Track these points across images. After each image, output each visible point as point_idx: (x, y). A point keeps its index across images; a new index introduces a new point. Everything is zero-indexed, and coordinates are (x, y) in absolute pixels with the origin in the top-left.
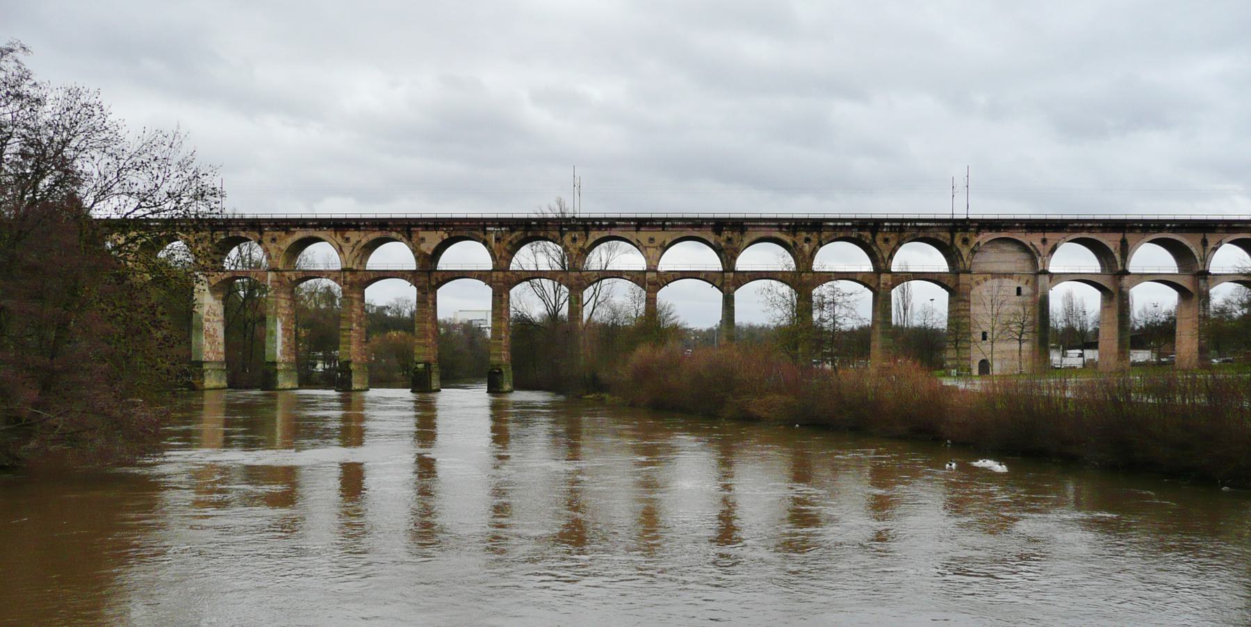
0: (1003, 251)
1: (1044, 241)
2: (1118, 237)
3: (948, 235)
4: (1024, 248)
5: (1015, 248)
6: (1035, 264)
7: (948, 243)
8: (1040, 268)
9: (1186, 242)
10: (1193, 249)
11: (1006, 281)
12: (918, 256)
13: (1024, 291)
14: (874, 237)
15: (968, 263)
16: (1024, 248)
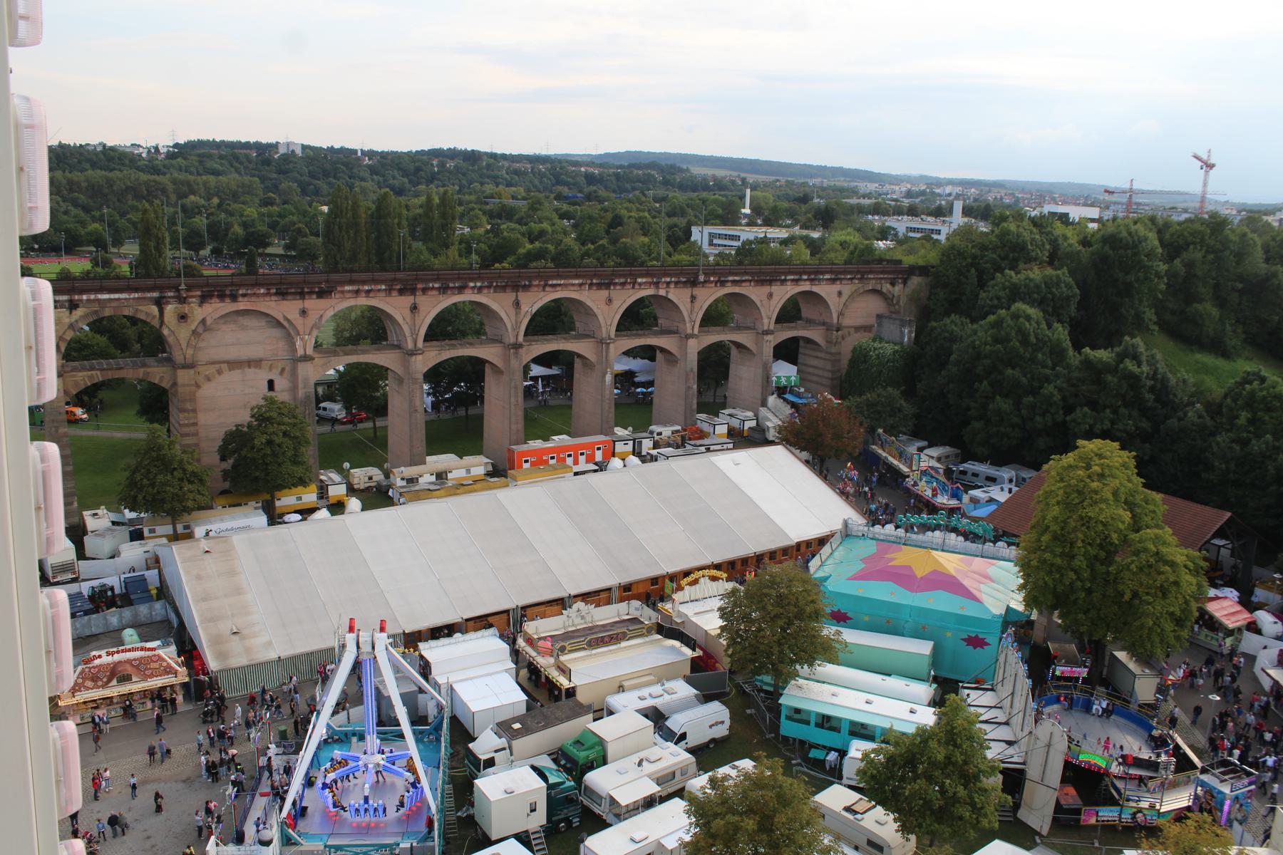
1: (304, 313)
2: (408, 300)
3: (154, 310)
4: (279, 324)
5: (263, 322)
6: (294, 350)
7: (156, 323)
8: (300, 352)
9: (494, 306)
10: (503, 315)
11: (251, 372)
13: (277, 387)
15: (190, 352)
16: (279, 324)
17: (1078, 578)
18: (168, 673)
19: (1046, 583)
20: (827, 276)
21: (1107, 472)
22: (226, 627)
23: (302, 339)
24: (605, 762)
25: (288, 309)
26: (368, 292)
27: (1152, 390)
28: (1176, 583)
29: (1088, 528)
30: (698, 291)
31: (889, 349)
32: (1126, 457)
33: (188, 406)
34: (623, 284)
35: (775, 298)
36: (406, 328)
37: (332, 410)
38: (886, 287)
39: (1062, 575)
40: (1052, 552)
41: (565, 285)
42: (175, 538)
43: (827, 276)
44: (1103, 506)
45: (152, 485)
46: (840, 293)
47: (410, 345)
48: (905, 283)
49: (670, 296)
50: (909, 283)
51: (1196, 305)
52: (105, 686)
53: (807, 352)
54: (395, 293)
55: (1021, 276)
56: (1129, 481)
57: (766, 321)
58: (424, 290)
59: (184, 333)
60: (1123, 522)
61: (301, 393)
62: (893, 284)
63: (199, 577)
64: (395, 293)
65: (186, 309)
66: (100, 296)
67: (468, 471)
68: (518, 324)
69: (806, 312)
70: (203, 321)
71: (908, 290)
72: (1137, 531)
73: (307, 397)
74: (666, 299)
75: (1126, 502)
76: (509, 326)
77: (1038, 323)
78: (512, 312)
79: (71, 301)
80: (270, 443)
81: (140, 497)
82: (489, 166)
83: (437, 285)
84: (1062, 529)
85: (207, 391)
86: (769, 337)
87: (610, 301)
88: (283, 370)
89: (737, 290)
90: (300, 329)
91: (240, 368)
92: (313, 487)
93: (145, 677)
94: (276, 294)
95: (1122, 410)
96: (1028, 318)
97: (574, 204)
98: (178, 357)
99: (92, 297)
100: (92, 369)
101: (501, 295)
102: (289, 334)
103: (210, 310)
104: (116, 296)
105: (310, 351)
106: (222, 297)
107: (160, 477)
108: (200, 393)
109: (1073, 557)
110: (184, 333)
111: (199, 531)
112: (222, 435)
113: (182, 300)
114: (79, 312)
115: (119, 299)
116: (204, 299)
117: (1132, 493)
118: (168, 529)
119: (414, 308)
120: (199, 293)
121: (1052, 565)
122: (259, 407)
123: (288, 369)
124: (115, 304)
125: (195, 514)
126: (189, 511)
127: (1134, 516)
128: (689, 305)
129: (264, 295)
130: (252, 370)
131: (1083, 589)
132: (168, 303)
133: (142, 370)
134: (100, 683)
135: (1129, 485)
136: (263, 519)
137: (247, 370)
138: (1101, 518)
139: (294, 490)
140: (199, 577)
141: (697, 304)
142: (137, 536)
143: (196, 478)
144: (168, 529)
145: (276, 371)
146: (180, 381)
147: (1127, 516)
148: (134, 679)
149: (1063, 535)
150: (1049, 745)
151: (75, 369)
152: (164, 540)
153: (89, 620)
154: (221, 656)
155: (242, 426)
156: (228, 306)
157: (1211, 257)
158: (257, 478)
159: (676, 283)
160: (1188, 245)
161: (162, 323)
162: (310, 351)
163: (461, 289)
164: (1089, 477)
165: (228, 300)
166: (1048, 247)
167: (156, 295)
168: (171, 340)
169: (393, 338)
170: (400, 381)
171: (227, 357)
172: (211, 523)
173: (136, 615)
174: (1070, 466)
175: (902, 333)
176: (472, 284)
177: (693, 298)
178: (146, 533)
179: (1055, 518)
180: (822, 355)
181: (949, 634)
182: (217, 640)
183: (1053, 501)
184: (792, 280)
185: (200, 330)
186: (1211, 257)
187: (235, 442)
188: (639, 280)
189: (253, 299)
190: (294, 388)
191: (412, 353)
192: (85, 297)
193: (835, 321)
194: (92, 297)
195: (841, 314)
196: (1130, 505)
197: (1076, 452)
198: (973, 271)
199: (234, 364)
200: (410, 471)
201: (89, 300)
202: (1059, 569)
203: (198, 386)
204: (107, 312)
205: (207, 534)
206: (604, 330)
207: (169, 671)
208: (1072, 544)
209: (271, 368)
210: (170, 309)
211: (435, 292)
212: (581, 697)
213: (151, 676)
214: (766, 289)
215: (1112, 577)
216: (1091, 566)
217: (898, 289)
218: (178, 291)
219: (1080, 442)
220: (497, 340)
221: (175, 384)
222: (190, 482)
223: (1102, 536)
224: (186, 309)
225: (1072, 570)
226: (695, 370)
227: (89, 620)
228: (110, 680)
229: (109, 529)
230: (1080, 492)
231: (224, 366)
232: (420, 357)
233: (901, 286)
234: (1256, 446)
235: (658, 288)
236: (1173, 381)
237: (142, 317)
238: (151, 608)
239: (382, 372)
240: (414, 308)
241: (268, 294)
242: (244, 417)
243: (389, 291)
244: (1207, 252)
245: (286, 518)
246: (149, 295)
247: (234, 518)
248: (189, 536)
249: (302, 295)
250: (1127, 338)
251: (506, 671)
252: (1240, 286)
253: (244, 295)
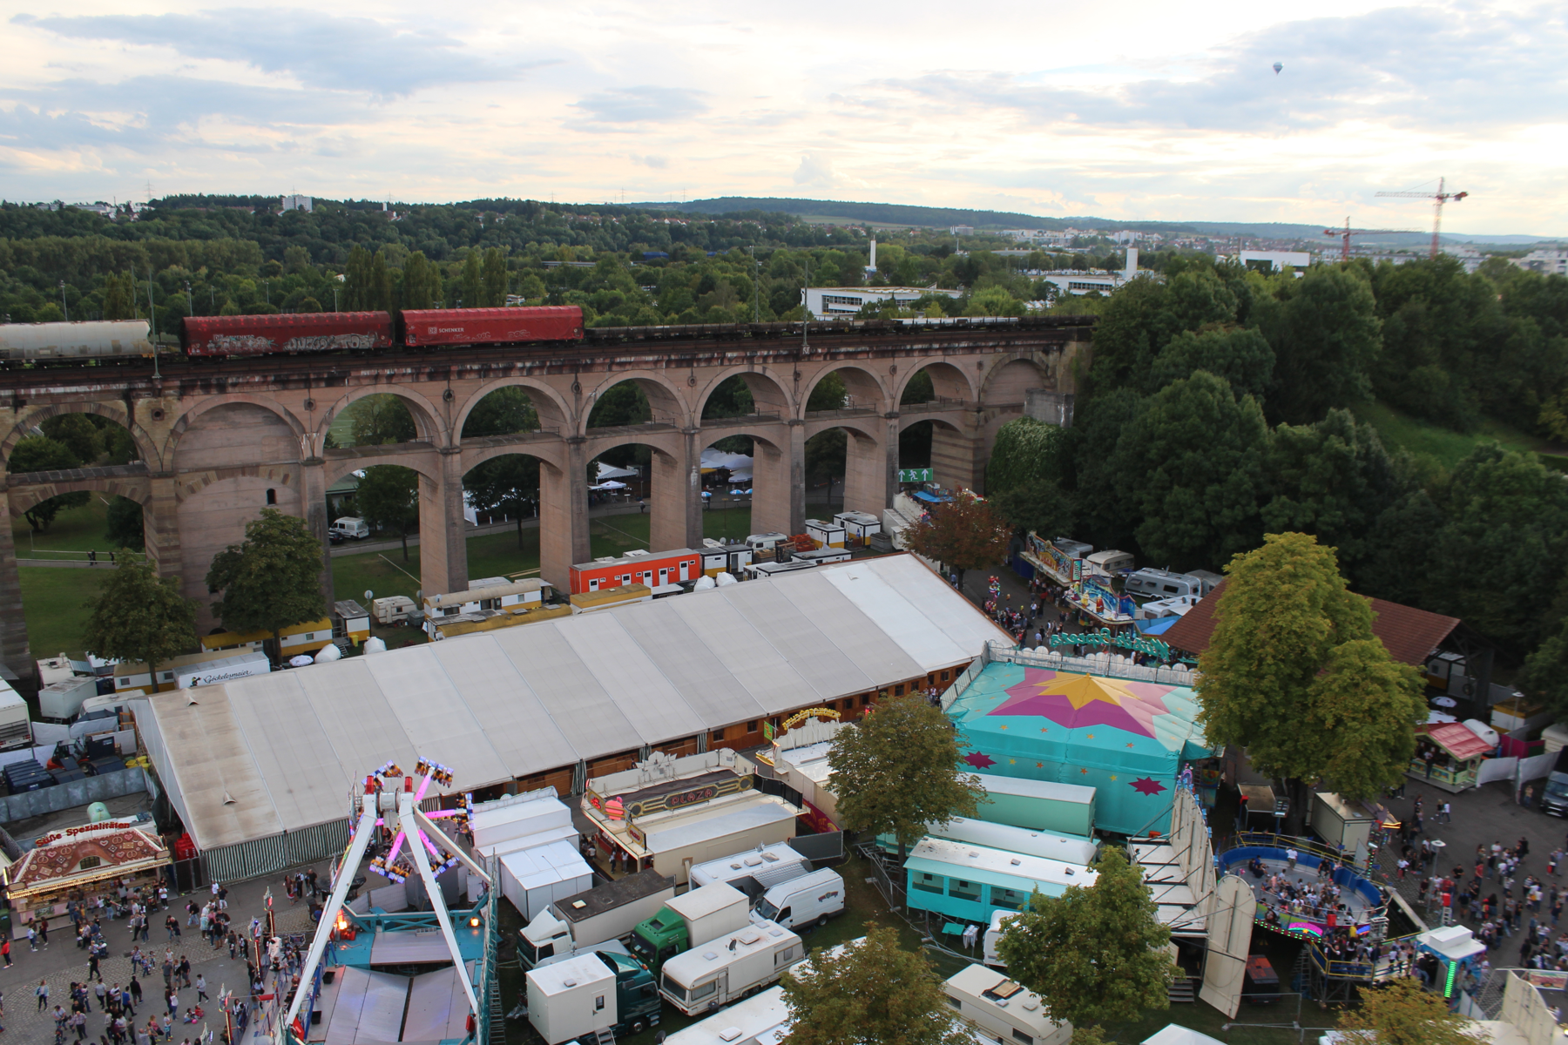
0: (235, 426)
1: (310, 405)
2: (440, 386)
3: (122, 405)
4: (278, 420)
5: (259, 418)
7: (124, 421)
8: (307, 454)
9: (549, 391)
10: (559, 401)
11: (245, 481)
13: (279, 497)
15: (168, 457)
16: (278, 420)
17: (1270, 703)
18: (145, 855)
19: (1230, 710)
20: (964, 344)
21: (1300, 571)
22: (217, 795)
23: (309, 438)
24: (689, 946)
25: (290, 401)
26: (390, 377)
27: (1364, 472)
28: (1387, 705)
29: (1279, 640)
30: (802, 367)
31: (1041, 433)
32: (1326, 552)
33: (168, 525)
34: (709, 360)
35: (900, 373)
36: (438, 421)
37: (351, 527)
38: (1038, 356)
39: (1250, 699)
40: (1237, 671)
41: (638, 363)
42: (155, 689)
43: (964, 344)
44: (1296, 613)
45: (124, 624)
46: (980, 365)
47: (444, 442)
48: (1061, 350)
49: (769, 374)
50: (1067, 350)
51: (1420, 368)
52: (65, 873)
53: (942, 438)
54: (423, 378)
55: (1203, 337)
56: (1329, 581)
57: (888, 401)
58: (461, 374)
59: (160, 434)
60: (1322, 632)
61: (308, 506)
62: (1046, 352)
63: (183, 736)
64: (423, 378)
65: (162, 404)
66: (52, 390)
67: (521, 597)
68: (579, 412)
69: (940, 390)
70: (184, 418)
71: (1065, 359)
72: (1338, 643)
73: (317, 510)
74: (763, 377)
75: (1325, 608)
76: (568, 416)
77: (1223, 394)
78: (571, 397)
79: (15, 397)
80: (270, 567)
81: (108, 639)
82: (548, 220)
83: (476, 367)
84: (1248, 642)
85: (192, 504)
86: (895, 422)
87: (693, 381)
88: (286, 477)
89: (851, 363)
90: (307, 425)
91: (232, 475)
92: (327, 622)
93: (116, 861)
94: (274, 382)
95: (1328, 499)
96: (1212, 389)
97: (655, 264)
98: (152, 464)
99: (43, 391)
100: (45, 481)
101: (557, 378)
102: (292, 432)
103: (192, 404)
104: (73, 389)
105: (319, 453)
106: (207, 388)
107: (134, 613)
108: (183, 508)
109: (1262, 677)
110: (160, 434)
111: (184, 680)
112: (211, 560)
113: (157, 393)
114: (26, 411)
115: (77, 393)
116: (184, 391)
117: (1333, 596)
118: (146, 679)
119: (448, 396)
120: (178, 383)
121: (1237, 687)
122: (257, 524)
123: (291, 476)
124: (70, 400)
125: (178, 659)
126: (171, 655)
127: (1336, 625)
128: (792, 384)
129: (258, 384)
130: (247, 478)
131: (1276, 716)
132: (139, 396)
133: (108, 482)
134: (59, 870)
135: (1330, 587)
136: (265, 663)
137: (240, 478)
138: (1294, 627)
139: (303, 626)
140: (183, 736)
141: (802, 383)
142: (105, 688)
143: (178, 614)
144: (146, 679)
145: (277, 479)
146: (155, 493)
147: (1326, 624)
148: (103, 863)
149: (1249, 651)
150: (1234, 907)
151: (23, 482)
152: (140, 693)
153: (46, 794)
154: (212, 831)
155: (236, 547)
156: (215, 399)
157: (1437, 308)
158: (256, 613)
159: (776, 357)
160: (1409, 294)
161: (132, 421)
162: (319, 453)
163: (506, 371)
164: (1279, 578)
165: (214, 391)
166: (1236, 301)
167: (123, 386)
168: (143, 442)
169: (423, 435)
170: (434, 487)
171: (215, 463)
172: (199, 669)
173: (105, 786)
174: (1256, 566)
175: (1058, 412)
176: (519, 365)
177: (797, 375)
178: (118, 685)
179: (1238, 629)
180: (961, 442)
181: (1114, 778)
182: (206, 813)
183: (1237, 609)
184: (921, 350)
185: (181, 430)
186: (1437, 308)
187: (228, 565)
188: (729, 355)
189: (246, 389)
190: (298, 501)
191: (447, 452)
192: (33, 391)
193: (975, 399)
194: (43, 391)
195: (982, 391)
196: (1330, 612)
197: (1263, 548)
198: (1144, 333)
199: (224, 472)
200: (451, 599)
201: (38, 395)
202: (1246, 691)
203: (179, 499)
204: (62, 410)
205: (195, 683)
206: (687, 417)
207: (147, 851)
208: (1261, 661)
209: (270, 475)
210: (141, 403)
211: (473, 376)
212: (659, 867)
213: (124, 859)
214: (887, 363)
215: (1310, 701)
216: (1284, 688)
217: (1052, 358)
218: (151, 381)
219: (1268, 537)
220: (554, 435)
221: (149, 498)
222: (171, 619)
223: (1298, 650)
224: (162, 404)
225: (1262, 692)
226: (803, 464)
227: (46, 794)
228: (72, 865)
229: (70, 681)
230: (1268, 597)
231: (212, 474)
232: (457, 458)
233: (1056, 354)
234: (1492, 538)
235: (752, 363)
236: (1390, 462)
237: (106, 414)
238: (124, 777)
239: (411, 477)
240: (448, 396)
241: (265, 383)
242: (239, 537)
243: (416, 376)
244: (1433, 302)
245: (293, 661)
246: (114, 387)
247: (228, 663)
248: (172, 686)
249: (307, 383)
250: (1332, 410)
251: (567, 839)
252: (1473, 343)
253: (234, 385)
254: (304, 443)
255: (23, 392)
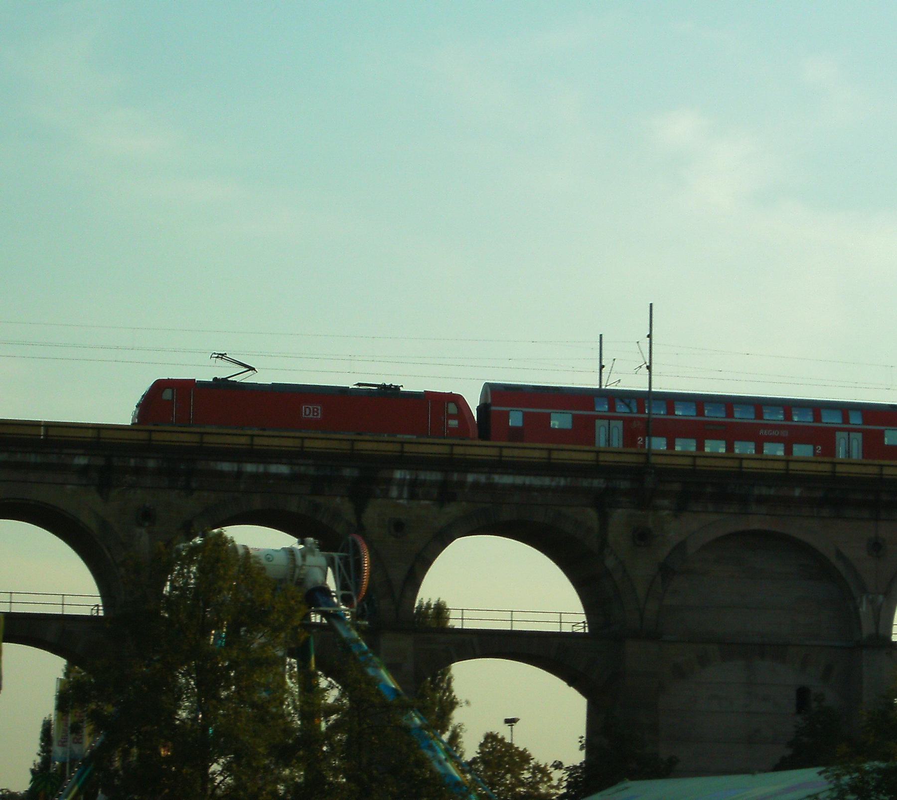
1: (876, 547)
3: (591, 516)
12: (492, 579)
14: (359, 511)
70: (681, 547)
99: (482, 478)
104: (528, 480)
167: (598, 483)
192: (470, 478)
201: (476, 485)
210: (619, 516)
246: (585, 483)
253: (761, 500)
254: (864, 608)
255: (455, 477)
